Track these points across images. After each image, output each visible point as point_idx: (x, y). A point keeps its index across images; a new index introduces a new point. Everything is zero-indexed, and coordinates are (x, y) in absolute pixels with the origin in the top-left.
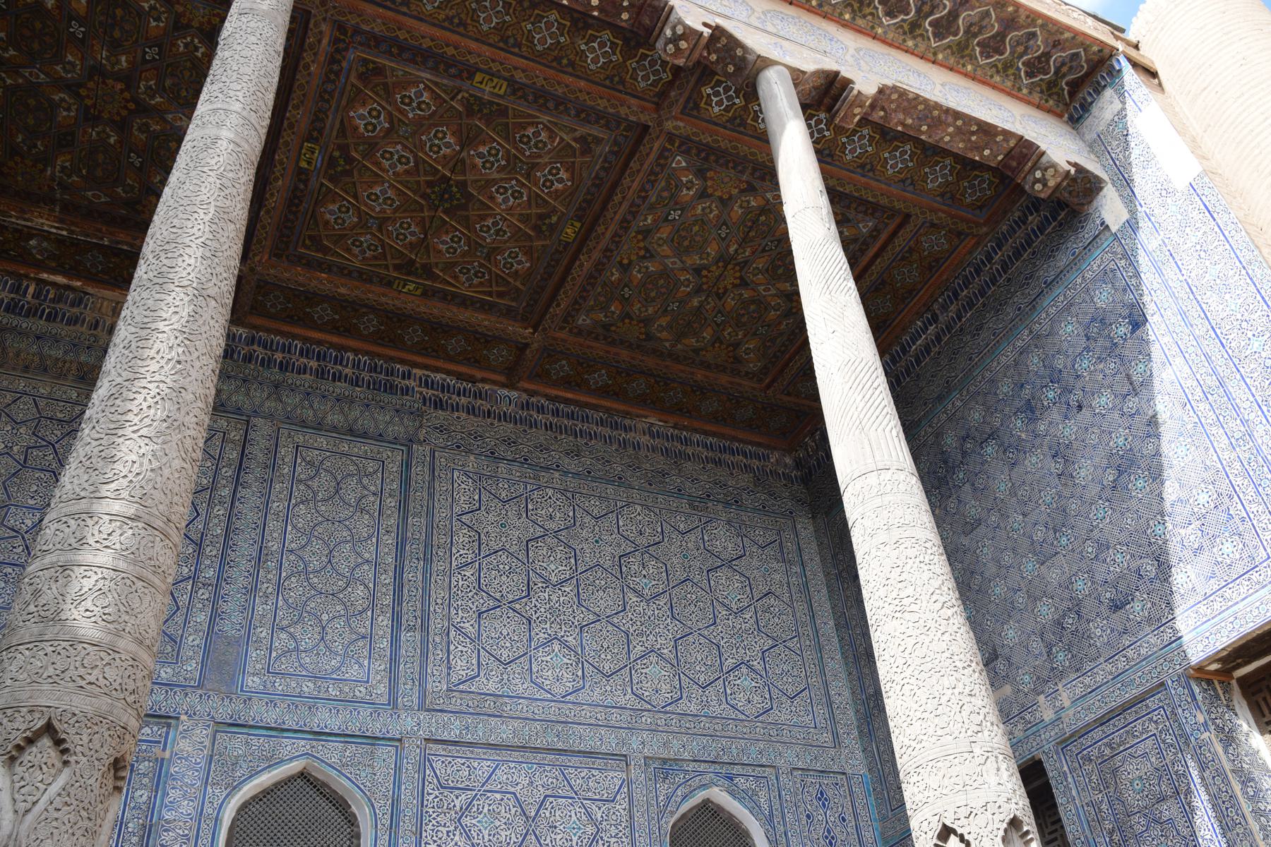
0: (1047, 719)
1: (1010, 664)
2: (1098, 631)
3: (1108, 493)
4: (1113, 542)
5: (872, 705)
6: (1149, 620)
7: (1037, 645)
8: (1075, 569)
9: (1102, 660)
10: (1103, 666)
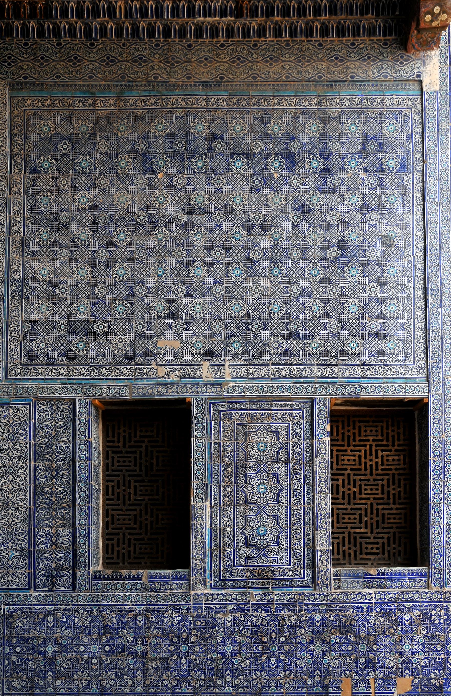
0: (205, 379)
1: (187, 328)
2: (276, 345)
3: (327, 262)
4: (315, 295)
5: (14, 287)
6: (318, 357)
7: (218, 328)
8: (277, 295)
9: (270, 363)
10: (269, 367)
